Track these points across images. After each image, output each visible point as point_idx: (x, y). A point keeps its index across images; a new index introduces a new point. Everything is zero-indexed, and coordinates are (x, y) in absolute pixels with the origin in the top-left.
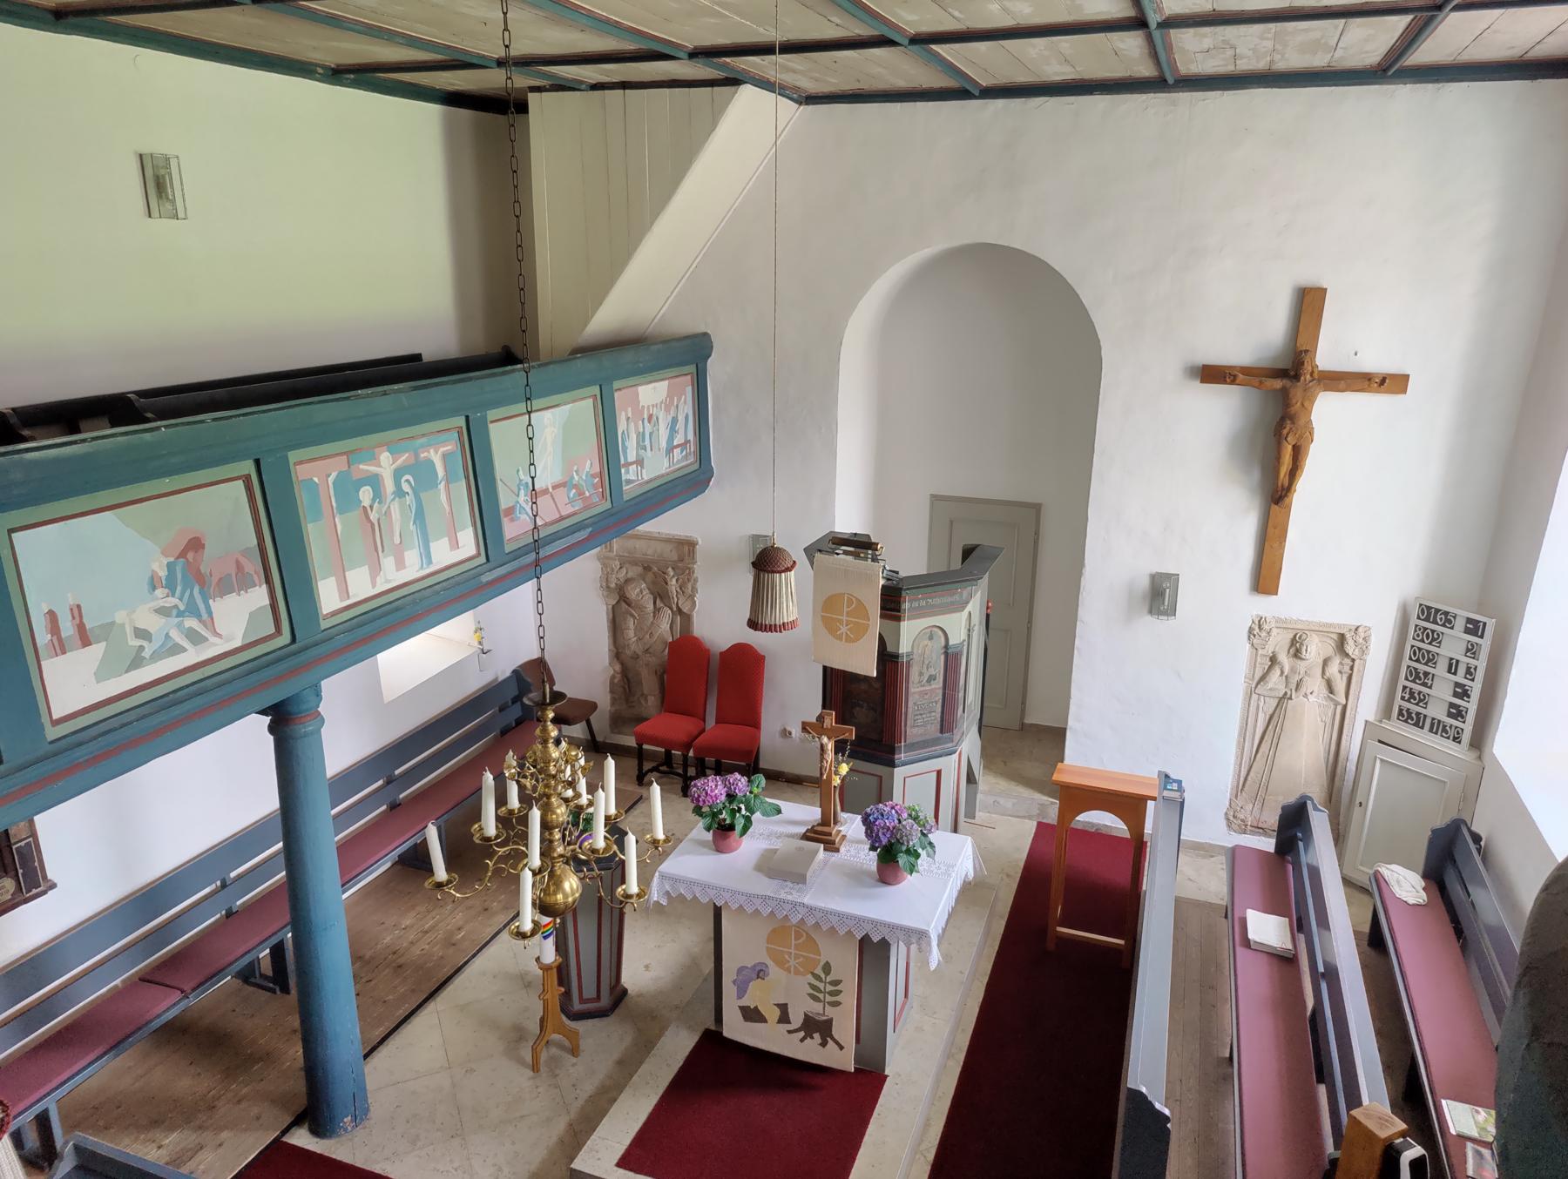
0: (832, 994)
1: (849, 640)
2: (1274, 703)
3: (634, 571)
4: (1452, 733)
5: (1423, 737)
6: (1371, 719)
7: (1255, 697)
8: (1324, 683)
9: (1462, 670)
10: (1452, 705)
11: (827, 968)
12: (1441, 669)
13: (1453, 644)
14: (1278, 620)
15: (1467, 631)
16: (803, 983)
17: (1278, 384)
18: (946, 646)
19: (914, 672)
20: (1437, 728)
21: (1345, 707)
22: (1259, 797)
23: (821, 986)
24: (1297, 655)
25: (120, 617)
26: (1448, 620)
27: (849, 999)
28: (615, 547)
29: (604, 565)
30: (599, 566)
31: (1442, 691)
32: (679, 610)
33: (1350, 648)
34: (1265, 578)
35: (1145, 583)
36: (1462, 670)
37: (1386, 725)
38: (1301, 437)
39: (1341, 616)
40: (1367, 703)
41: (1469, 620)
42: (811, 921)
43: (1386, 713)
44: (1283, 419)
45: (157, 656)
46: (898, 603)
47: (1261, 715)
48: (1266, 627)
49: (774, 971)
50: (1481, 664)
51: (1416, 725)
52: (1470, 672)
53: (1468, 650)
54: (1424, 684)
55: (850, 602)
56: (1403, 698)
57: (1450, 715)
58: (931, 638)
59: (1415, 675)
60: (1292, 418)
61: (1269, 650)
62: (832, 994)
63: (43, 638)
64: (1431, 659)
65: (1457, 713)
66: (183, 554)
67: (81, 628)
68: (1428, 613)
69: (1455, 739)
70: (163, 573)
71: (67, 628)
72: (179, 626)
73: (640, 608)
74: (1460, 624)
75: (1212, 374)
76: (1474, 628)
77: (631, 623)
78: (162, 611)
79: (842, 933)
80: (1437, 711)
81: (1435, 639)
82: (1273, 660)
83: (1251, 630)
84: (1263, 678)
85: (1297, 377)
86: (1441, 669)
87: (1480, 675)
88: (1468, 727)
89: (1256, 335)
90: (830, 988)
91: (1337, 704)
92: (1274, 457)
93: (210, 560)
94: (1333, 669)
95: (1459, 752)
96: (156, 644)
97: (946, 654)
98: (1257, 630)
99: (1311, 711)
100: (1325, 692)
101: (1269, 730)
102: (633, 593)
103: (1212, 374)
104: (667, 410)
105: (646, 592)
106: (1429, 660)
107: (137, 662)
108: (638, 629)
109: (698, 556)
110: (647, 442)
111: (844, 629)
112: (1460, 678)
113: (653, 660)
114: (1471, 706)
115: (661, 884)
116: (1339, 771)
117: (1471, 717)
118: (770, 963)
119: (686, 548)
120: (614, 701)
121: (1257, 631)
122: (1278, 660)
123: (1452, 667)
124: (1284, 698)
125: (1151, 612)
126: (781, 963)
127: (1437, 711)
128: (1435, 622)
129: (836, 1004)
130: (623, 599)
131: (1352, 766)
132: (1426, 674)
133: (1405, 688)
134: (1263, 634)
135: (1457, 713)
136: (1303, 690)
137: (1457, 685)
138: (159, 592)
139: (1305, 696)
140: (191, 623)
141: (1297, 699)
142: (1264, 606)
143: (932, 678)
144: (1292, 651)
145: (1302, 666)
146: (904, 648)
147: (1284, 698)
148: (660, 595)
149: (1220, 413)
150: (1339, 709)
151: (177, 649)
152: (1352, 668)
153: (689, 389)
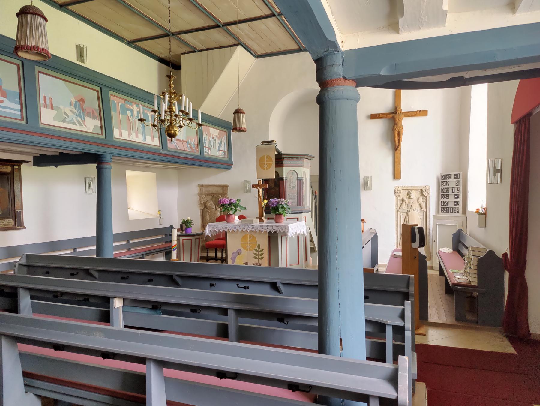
0: (261, 255)
1: (267, 169)
5: (449, 214)
8: (419, 206)
10: (455, 202)
11: (259, 247)
12: (450, 192)
13: (452, 184)
14: (403, 187)
15: (455, 178)
16: (252, 254)
17: (391, 115)
18: (298, 178)
19: (288, 184)
20: (453, 210)
23: (257, 253)
24: (409, 198)
25: (62, 107)
26: (449, 176)
27: (266, 255)
29: (200, 197)
31: (452, 199)
33: (424, 193)
34: (396, 175)
39: (420, 183)
40: (432, 210)
41: (455, 175)
42: (254, 230)
43: (438, 212)
44: (394, 126)
45: (69, 122)
46: (282, 161)
47: (402, 219)
48: (399, 189)
49: (244, 252)
50: (460, 186)
51: (447, 212)
54: (447, 199)
55: (267, 157)
57: (455, 205)
58: (293, 174)
62: (261, 255)
63: (42, 101)
64: (447, 190)
65: (457, 203)
66: (79, 101)
67: (52, 104)
70: (74, 103)
71: (48, 103)
72: (76, 118)
74: (453, 177)
75: (374, 116)
77: (208, 214)
78: (72, 111)
79: (263, 232)
80: (451, 205)
81: (446, 183)
82: (403, 200)
83: (395, 192)
84: (400, 206)
85: (396, 113)
86: (450, 192)
87: (461, 190)
88: (460, 207)
90: (260, 253)
91: (423, 212)
93: (86, 105)
94: (421, 200)
95: (460, 215)
96: (70, 119)
97: (298, 180)
98: (397, 191)
100: (419, 208)
102: (208, 204)
103: (374, 116)
104: (219, 138)
107: (64, 121)
108: (210, 216)
109: (229, 190)
110: (212, 144)
111: (266, 166)
112: (456, 193)
114: (460, 200)
115: (209, 228)
117: (460, 204)
118: (242, 249)
122: (404, 198)
123: (453, 191)
124: (408, 212)
126: (245, 248)
129: (262, 258)
131: (431, 232)
132: (447, 195)
135: (457, 203)
136: (413, 208)
138: (72, 106)
140: (79, 119)
141: (412, 212)
142: (397, 183)
143: (293, 187)
145: (411, 201)
146: (284, 176)
151: (74, 124)
153: (225, 136)
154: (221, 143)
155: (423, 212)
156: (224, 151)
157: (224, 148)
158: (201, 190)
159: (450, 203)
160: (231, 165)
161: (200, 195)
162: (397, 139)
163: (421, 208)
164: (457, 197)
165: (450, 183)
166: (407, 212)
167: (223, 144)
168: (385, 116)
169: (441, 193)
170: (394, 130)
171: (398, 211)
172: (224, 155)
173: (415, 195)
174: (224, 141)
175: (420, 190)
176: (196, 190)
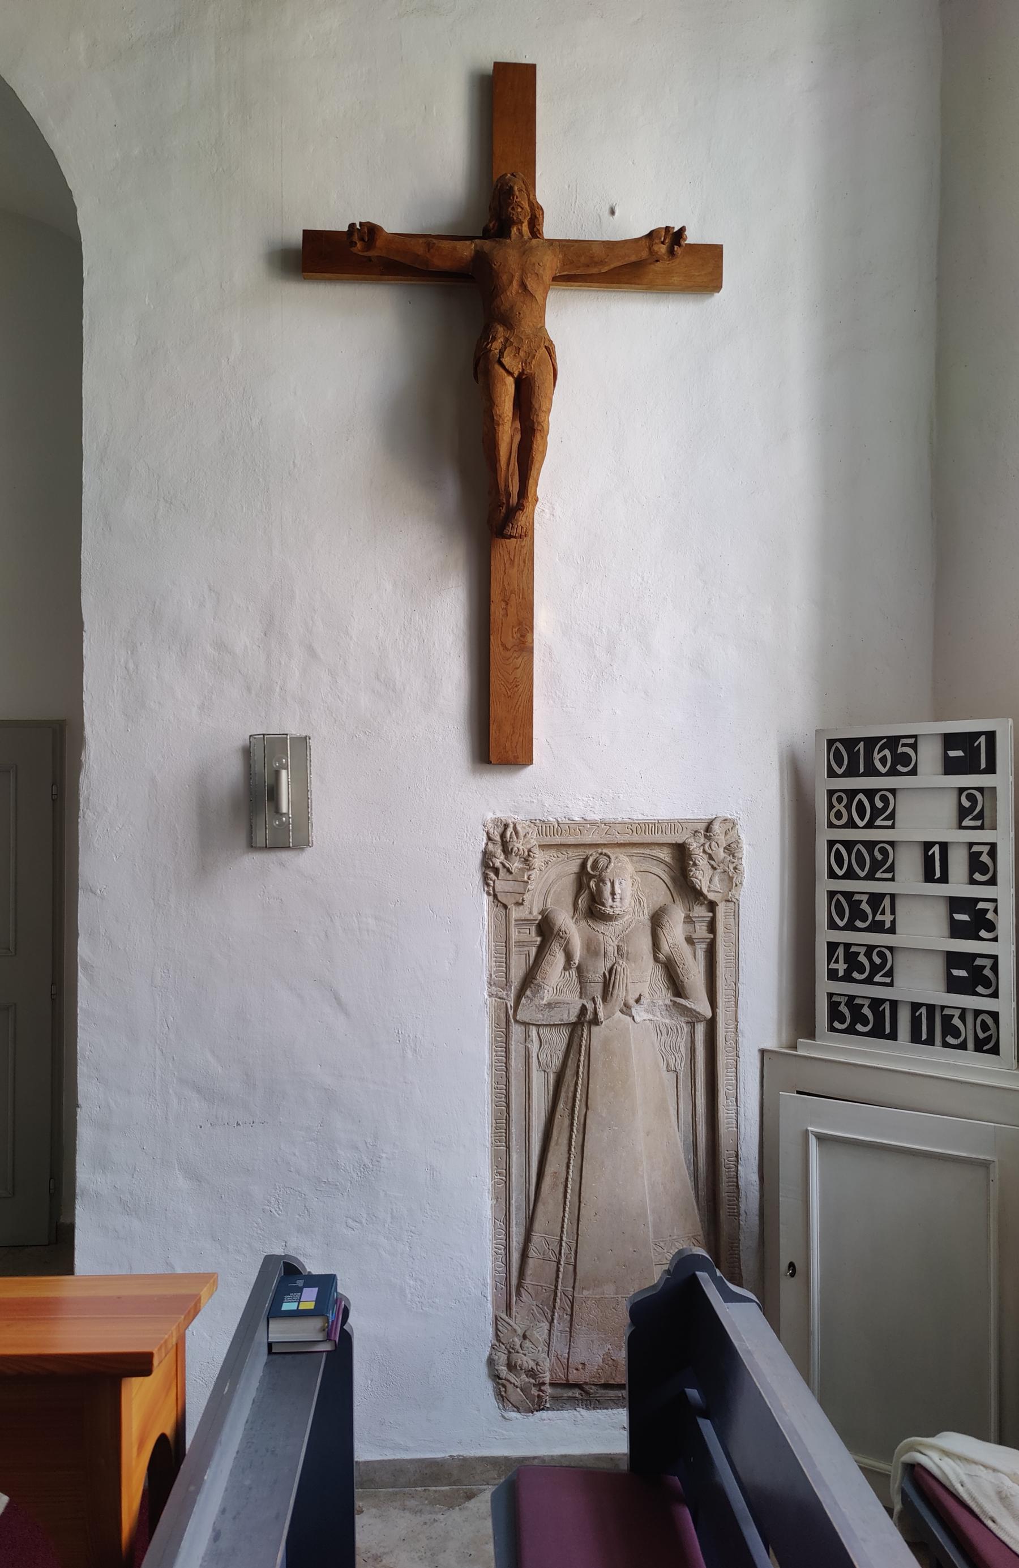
2: (559, 1040)
4: (968, 1031)
5: (900, 1056)
7: (516, 1030)
8: (659, 973)
9: (958, 864)
10: (953, 959)
12: (908, 877)
13: (924, 809)
14: (543, 827)
15: (951, 767)
20: (931, 1026)
21: (711, 1025)
22: (561, 1302)
31: (921, 930)
33: (703, 877)
34: (498, 732)
36: (958, 864)
37: (806, 1049)
38: (531, 355)
41: (950, 740)
43: (802, 1022)
44: (486, 335)
47: (537, 1079)
48: (519, 845)
51: (877, 1032)
52: (981, 866)
53: (963, 813)
54: (877, 927)
56: (833, 975)
57: (954, 986)
59: (850, 911)
60: (508, 322)
61: (533, 908)
64: (878, 860)
65: (970, 975)
68: (849, 754)
69: (979, 1047)
74: (929, 757)
76: (968, 753)
80: (919, 983)
81: (879, 808)
82: (546, 929)
83: (487, 857)
84: (530, 980)
86: (908, 877)
91: (692, 1017)
92: (477, 454)
94: (675, 932)
98: (500, 857)
99: (642, 1039)
100: (664, 996)
101: (554, 1115)
106: (876, 865)
112: (959, 887)
116: (724, 1186)
123: (934, 863)
124: (584, 1022)
125: (252, 846)
127: (919, 983)
128: (875, 773)
131: (749, 1174)
132: (876, 900)
133: (832, 947)
135: (970, 975)
136: (620, 994)
137: (956, 904)
139: (626, 1010)
145: (609, 935)
149: (352, 350)
150: (700, 1029)
152: (712, 927)
155: (692, 1017)
159: (902, 966)
162: (507, 434)
163: (676, 986)
164: (971, 919)
165: (905, 809)
169: (824, 885)
170: (481, 368)
171: (506, 1021)
173: (633, 889)
175: (665, 855)
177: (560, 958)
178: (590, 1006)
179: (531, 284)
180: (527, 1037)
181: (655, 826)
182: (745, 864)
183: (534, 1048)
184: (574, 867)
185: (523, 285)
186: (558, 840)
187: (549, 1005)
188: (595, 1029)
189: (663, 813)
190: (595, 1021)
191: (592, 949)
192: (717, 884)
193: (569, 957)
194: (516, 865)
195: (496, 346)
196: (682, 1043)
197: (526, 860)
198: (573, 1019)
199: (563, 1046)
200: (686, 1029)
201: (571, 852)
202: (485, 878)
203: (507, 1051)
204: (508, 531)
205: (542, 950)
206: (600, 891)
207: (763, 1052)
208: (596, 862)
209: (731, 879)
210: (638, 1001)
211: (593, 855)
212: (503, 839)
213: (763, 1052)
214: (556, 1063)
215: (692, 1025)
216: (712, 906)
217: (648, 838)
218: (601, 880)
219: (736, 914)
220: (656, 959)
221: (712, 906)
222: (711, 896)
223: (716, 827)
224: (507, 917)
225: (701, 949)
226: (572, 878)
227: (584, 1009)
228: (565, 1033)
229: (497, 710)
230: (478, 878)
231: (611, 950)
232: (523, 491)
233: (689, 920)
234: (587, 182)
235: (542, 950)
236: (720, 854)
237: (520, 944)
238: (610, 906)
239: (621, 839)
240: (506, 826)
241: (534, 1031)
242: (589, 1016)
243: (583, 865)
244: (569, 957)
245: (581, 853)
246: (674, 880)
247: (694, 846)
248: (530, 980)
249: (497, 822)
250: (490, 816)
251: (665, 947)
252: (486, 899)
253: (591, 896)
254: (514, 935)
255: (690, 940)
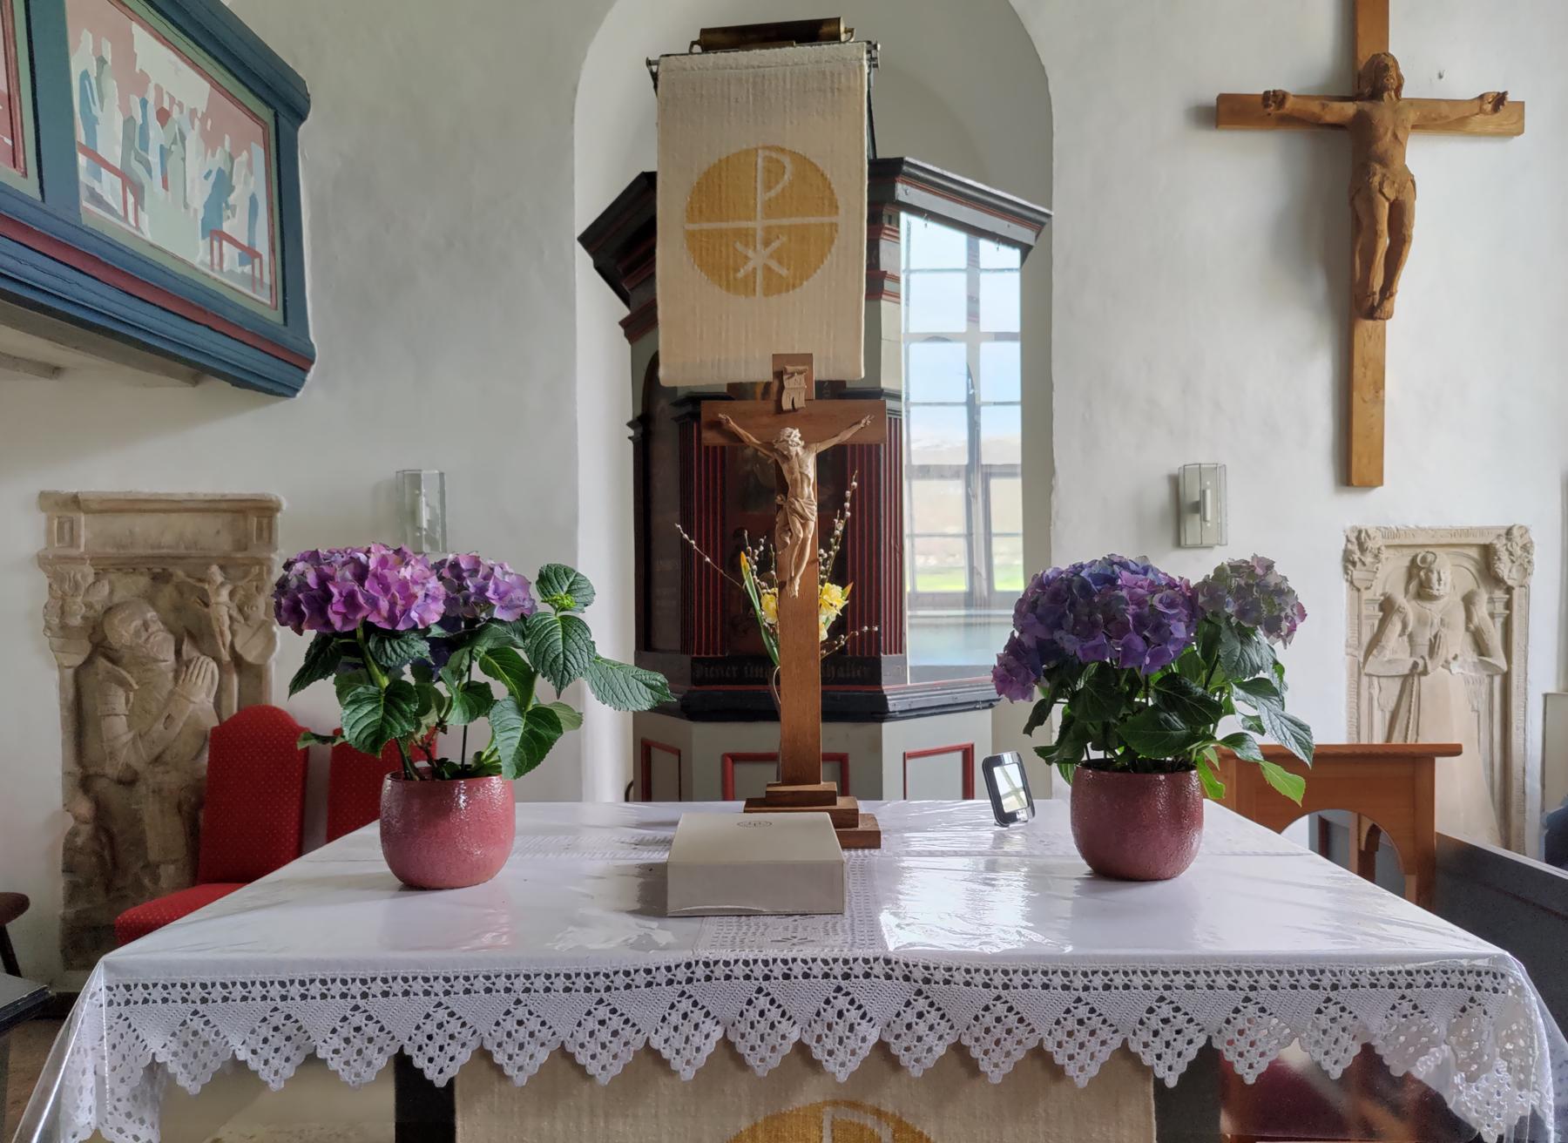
2: (1395, 686)
3: (130, 586)
6: (1552, 689)
7: (1365, 680)
8: (1468, 639)
14: (1387, 533)
21: (1507, 678)
28: (84, 535)
29: (57, 578)
30: (42, 580)
32: (237, 660)
33: (1504, 569)
34: (1354, 463)
35: (1160, 494)
39: (1474, 509)
47: (1377, 715)
48: (1370, 544)
60: (1384, 161)
61: (1376, 592)
73: (144, 663)
75: (1230, 112)
77: (119, 700)
84: (1375, 642)
89: (1295, 48)
94: (1482, 611)
98: (1357, 552)
100: (1472, 657)
102: (123, 632)
103: (1230, 112)
105: (156, 626)
113: (172, 780)
119: (253, 521)
120: (74, 892)
121: (1357, 556)
124: (1417, 672)
125: (1178, 543)
130: (101, 647)
134: (1369, 559)
136: (1444, 652)
139: (1446, 665)
141: (1437, 672)
144: (1413, 586)
145: (1434, 610)
147: (1417, 672)
148: (193, 632)
150: (1497, 680)
152: (1508, 605)
153: (259, 153)
154: (223, 184)
155: (1491, 669)
156: (249, 253)
157: (247, 219)
158: (66, 532)
160: (303, 361)
161: (54, 565)
163: (1481, 647)
166: (1405, 678)
167: (239, 197)
168: (1315, 107)
171: (1359, 672)
172: (254, 281)
173: (1452, 577)
174: (251, 179)
175: (1474, 553)
176: (28, 534)
177: (1398, 627)
178: (1421, 662)
179: (1400, 135)
180: (1370, 685)
181: (1468, 532)
182: (1535, 558)
183: (1376, 692)
184: (1406, 562)
185: (1395, 136)
186: (1397, 542)
187: (1389, 661)
188: (1423, 678)
189: (1474, 521)
190: (1425, 672)
191: (1422, 621)
192: (1514, 574)
193: (1405, 626)
194: (1369, 559)
195: (1376, 179)
196: (1484, 689)
197: (1376, 556)
198: (1406, 672)
199: (1397, 693)
200: (1487, 680)
201: (1406, 551)
202: (1346, 570)
203: (1358, 694)
204: (1377, 314)
205: (1383, 622)
206: (1429, 580)
207: (1546, 696)
208: (1424, 560)
209: (1525, 571)
210: (1455, 658)
211: (1421, 553)
212: (1360, 539)
213: (1546, 696)
214: (1392, 705)
215: (1491, 677)
216: (1509, 590)
217: (1464, 540)
218: (1430, 570)
219: (1527, 596)
220: (1467, 629)
221: (1509, 590)
222: (1510, 582)
223: (1515, 532)
224: (1359, 598)
225: (1499, 621)
226: (1404, 570)
227: (1415, 665)
228: (1397, 684)
229: (1357, 446)
230: (1340, 569)
231: (1437, 621)
232: (1388, 289)
233: (1491, 601)
234: (1433, 54)
235: (1383, 622)
236: (1518, 551)
237: (1368, 617)
238: (1436, 589)
239: (1444, 541)
240: (1360, 532)
241: (1375, 680)
242: (1420, 668)
243: (1413, 561)
244: (1405, 626)
245: (1412, 552)
246: (1479, 571)
247: (1500, 545)
248: (1375, 642)
249: (1353, 529)
250: (1348, 525)
251: (1476, 620)
252: (1345, 585)
253: (1420, 581)
254: (1364, 612)
255: (1492, 616)
